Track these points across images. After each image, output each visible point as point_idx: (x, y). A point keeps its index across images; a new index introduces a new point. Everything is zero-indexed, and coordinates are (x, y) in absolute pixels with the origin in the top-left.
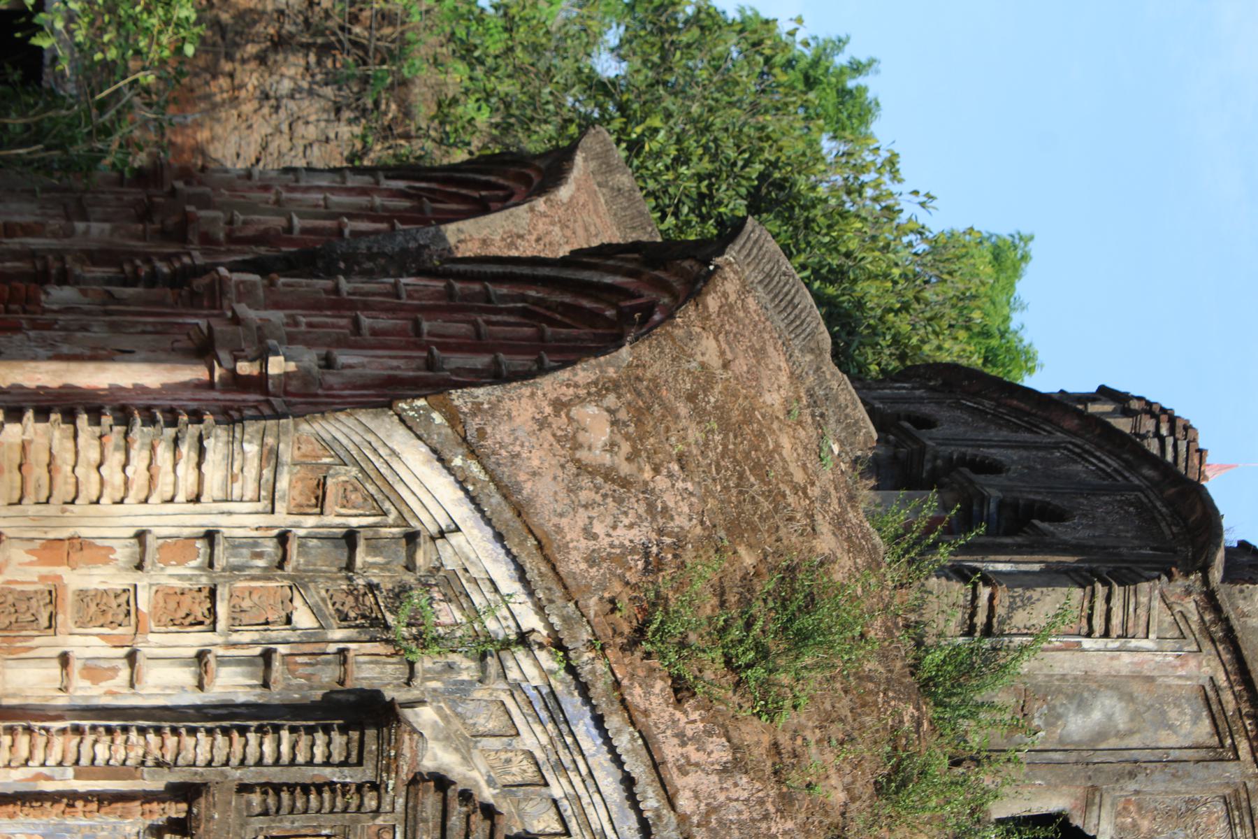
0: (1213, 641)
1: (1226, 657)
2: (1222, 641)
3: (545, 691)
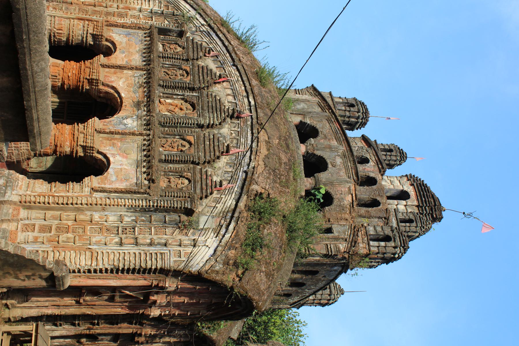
0: (317, 96)
1: (320, 97)
2: (318, 95)
3: (207, 32)
